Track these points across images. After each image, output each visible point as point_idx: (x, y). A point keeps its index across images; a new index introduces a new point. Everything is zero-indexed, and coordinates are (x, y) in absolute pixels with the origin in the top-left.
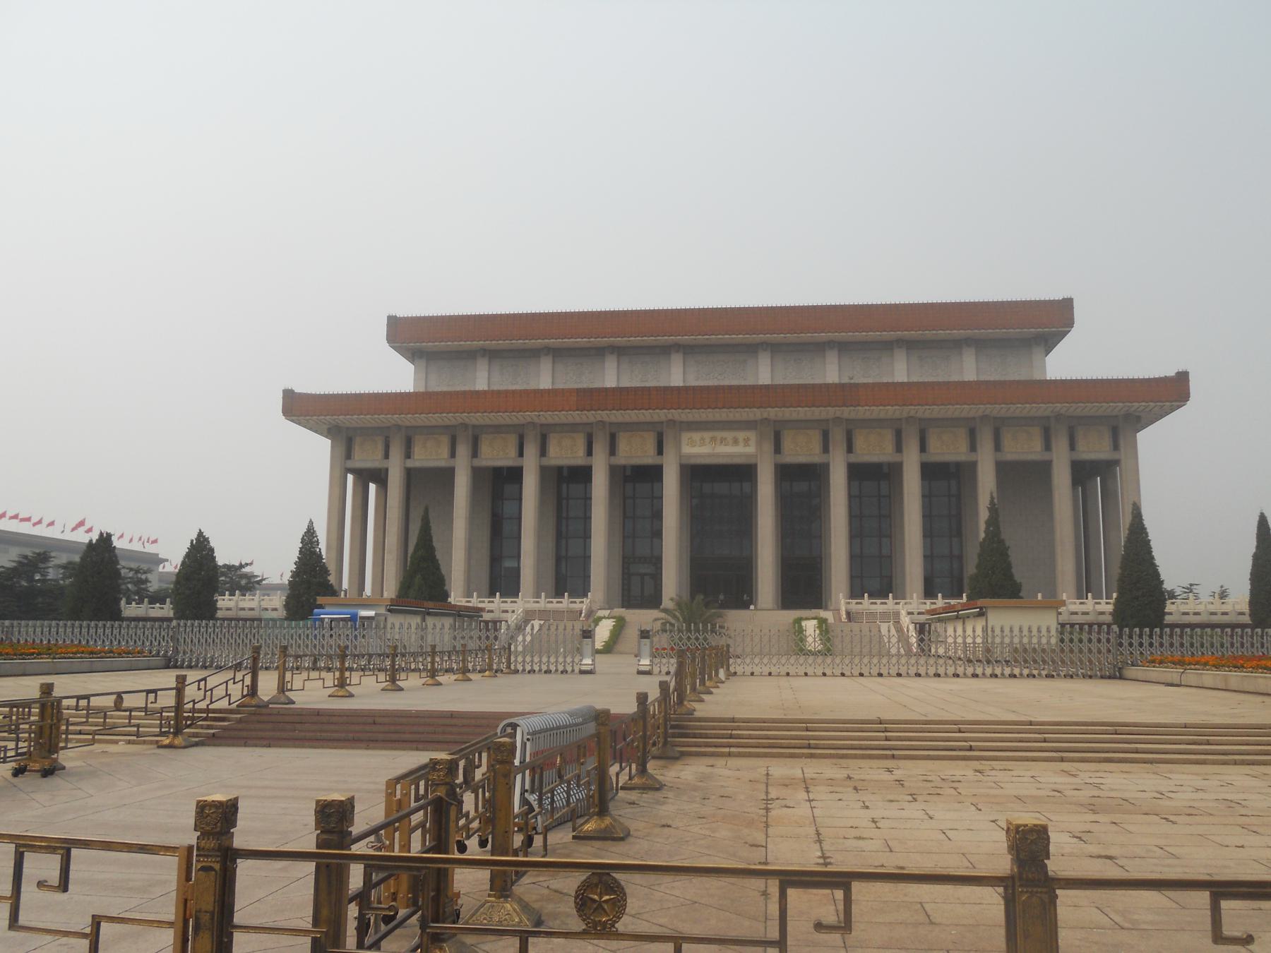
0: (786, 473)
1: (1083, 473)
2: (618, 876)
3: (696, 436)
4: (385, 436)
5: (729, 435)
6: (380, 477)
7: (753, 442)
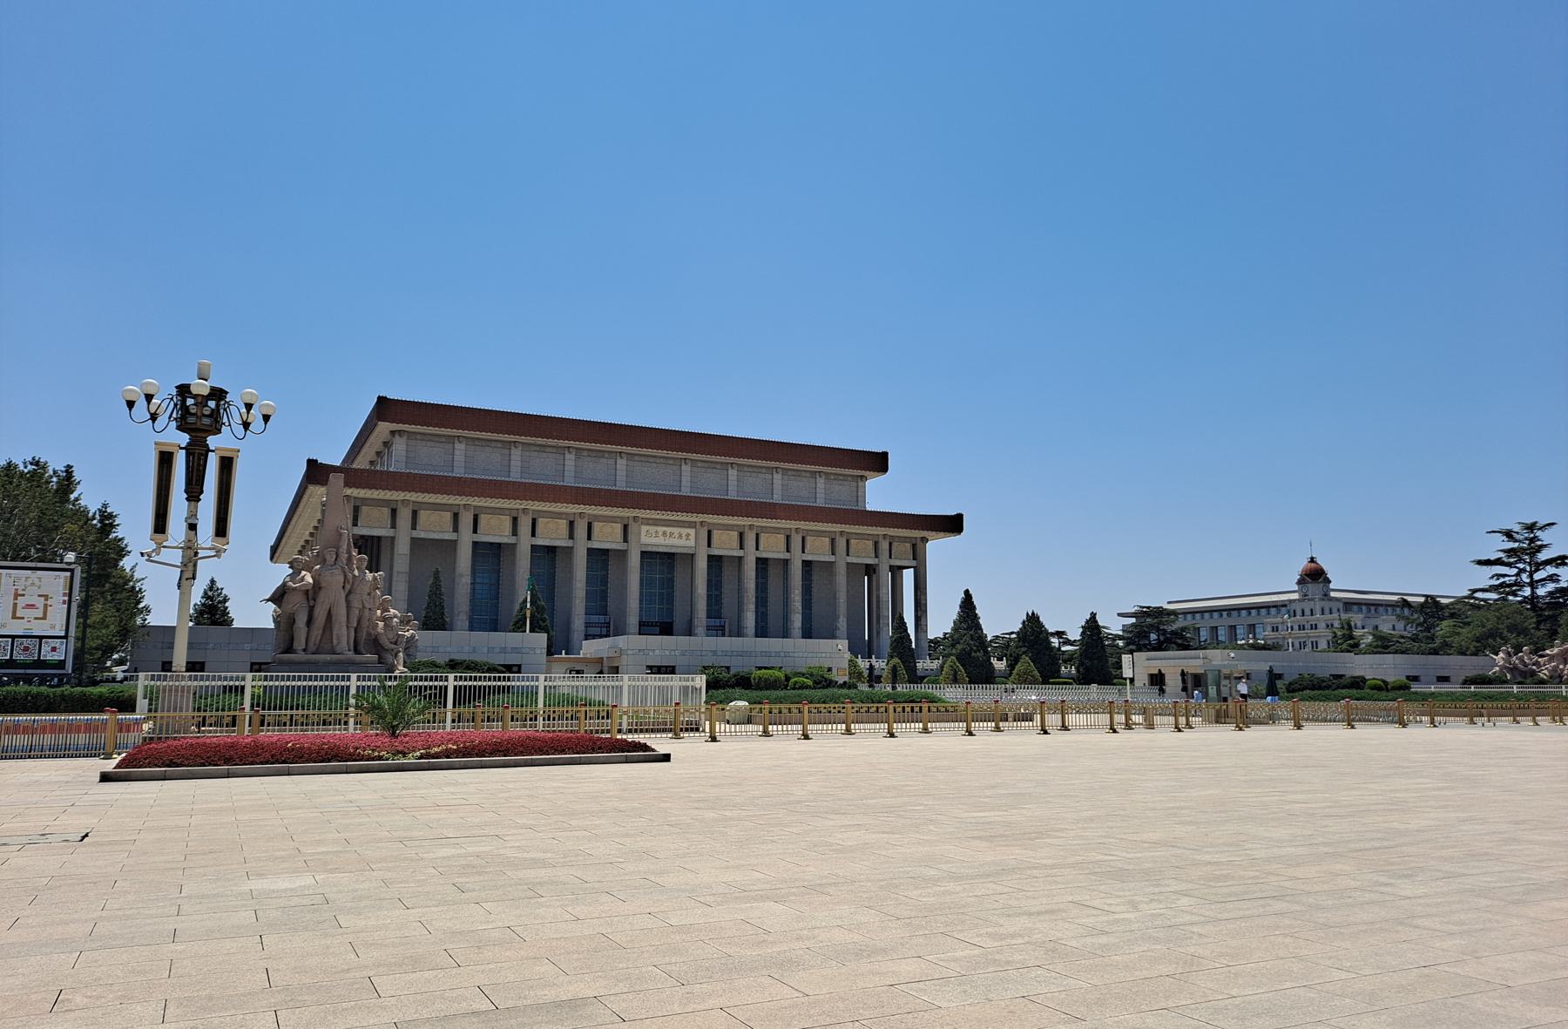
3: (653, 529)
5: (676, 531)
7: (692, 537)
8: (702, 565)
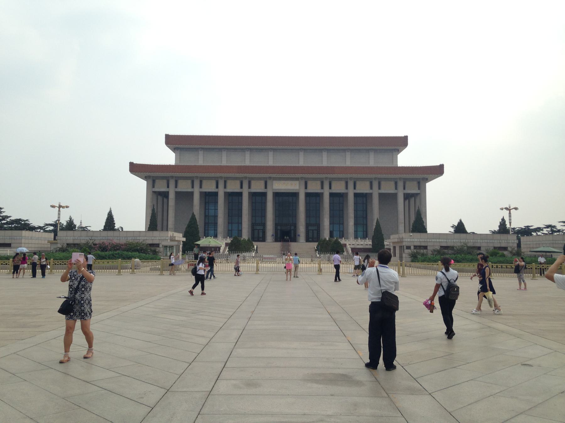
0: (308, 195)
1: (407, 197)
2: (445, 289)
4: (168, 179)
5: (290, 182)
6: (165, 195)
8: (302, 197)
